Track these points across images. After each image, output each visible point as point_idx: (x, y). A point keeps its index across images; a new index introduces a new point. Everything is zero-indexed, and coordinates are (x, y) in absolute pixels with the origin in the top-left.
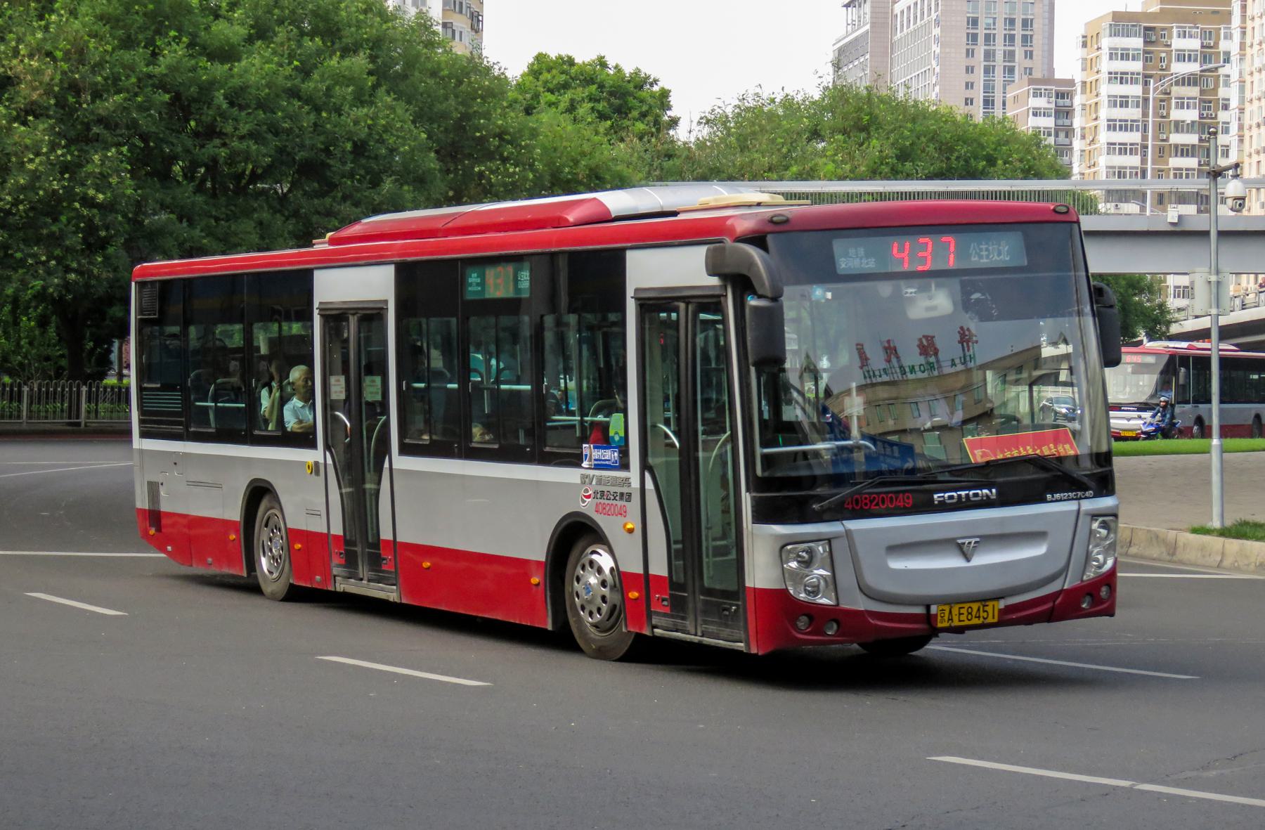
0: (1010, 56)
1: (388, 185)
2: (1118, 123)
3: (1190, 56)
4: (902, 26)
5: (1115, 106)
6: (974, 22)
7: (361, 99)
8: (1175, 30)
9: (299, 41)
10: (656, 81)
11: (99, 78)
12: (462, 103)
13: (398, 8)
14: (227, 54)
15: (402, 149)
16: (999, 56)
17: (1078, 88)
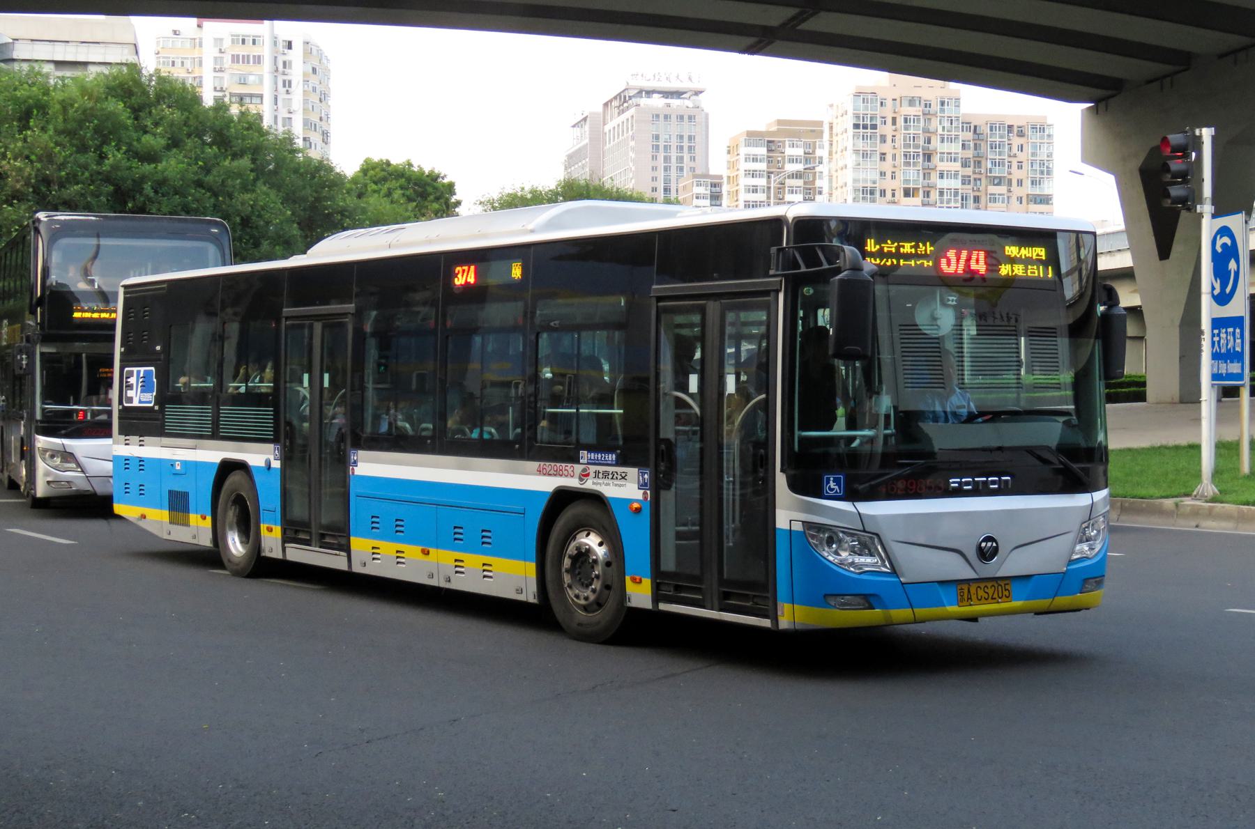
0: (680, 159)
1: (265, 245)
2: (751, 204)
3: (796, 159)
4: (610, 140)
5: (749, 192)
6: (657, 137)
7: (245, 188)
8: (787, 143)
9: (202, 148)
10: (445, 176)
11: (63, 173)
12: (316, 192)
13: (270, 127)
14: (150, 157)
15: (274, 222)
16: (674, 159)
17: (725, 180)
